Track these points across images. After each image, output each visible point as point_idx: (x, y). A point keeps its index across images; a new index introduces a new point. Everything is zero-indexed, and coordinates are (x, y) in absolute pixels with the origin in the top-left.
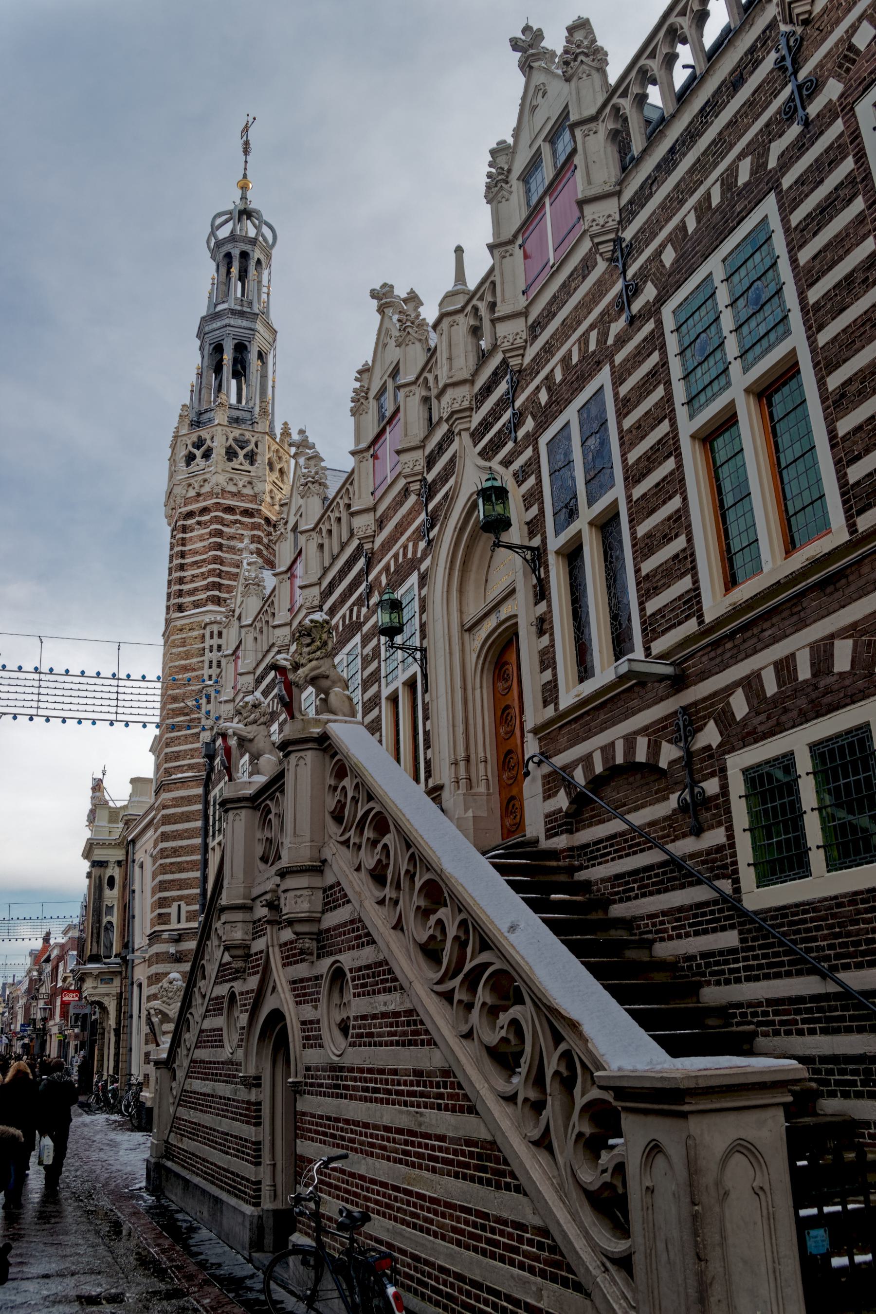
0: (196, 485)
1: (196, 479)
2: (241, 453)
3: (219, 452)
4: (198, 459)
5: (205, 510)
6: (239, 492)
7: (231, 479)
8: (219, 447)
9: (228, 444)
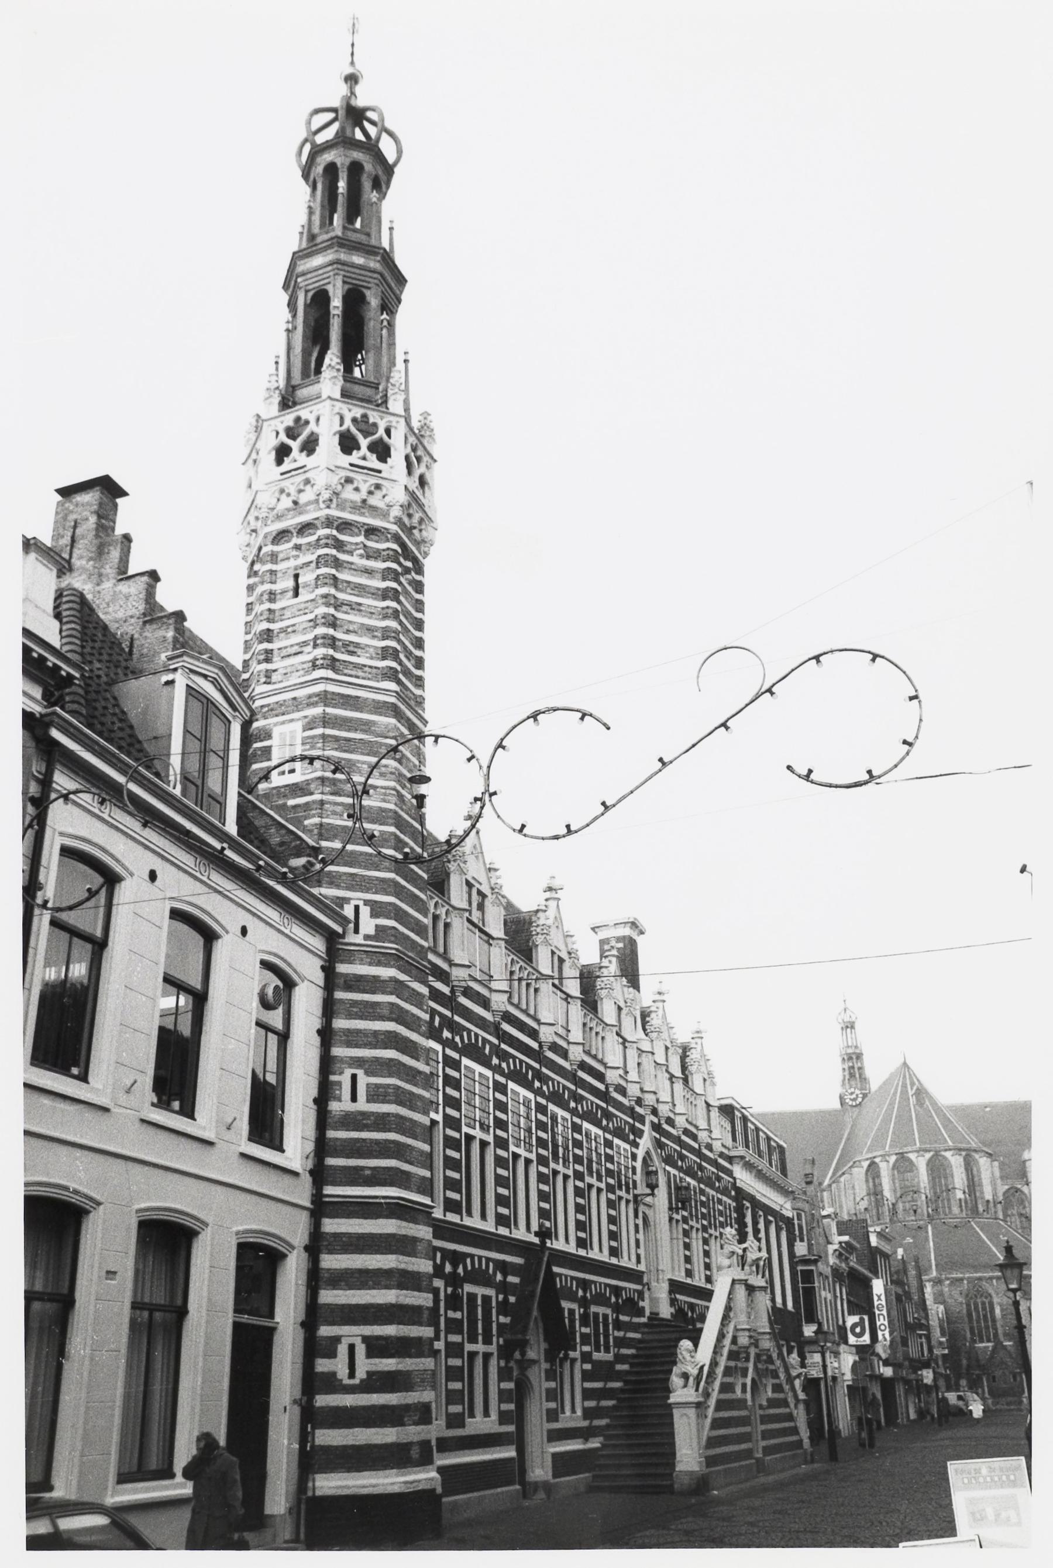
0: (292, 490)
1: (292, 480)
2: (364, 443)
4: (295, 453)
5: (305, 528)
6: (364, 501)
7: (349, 480)
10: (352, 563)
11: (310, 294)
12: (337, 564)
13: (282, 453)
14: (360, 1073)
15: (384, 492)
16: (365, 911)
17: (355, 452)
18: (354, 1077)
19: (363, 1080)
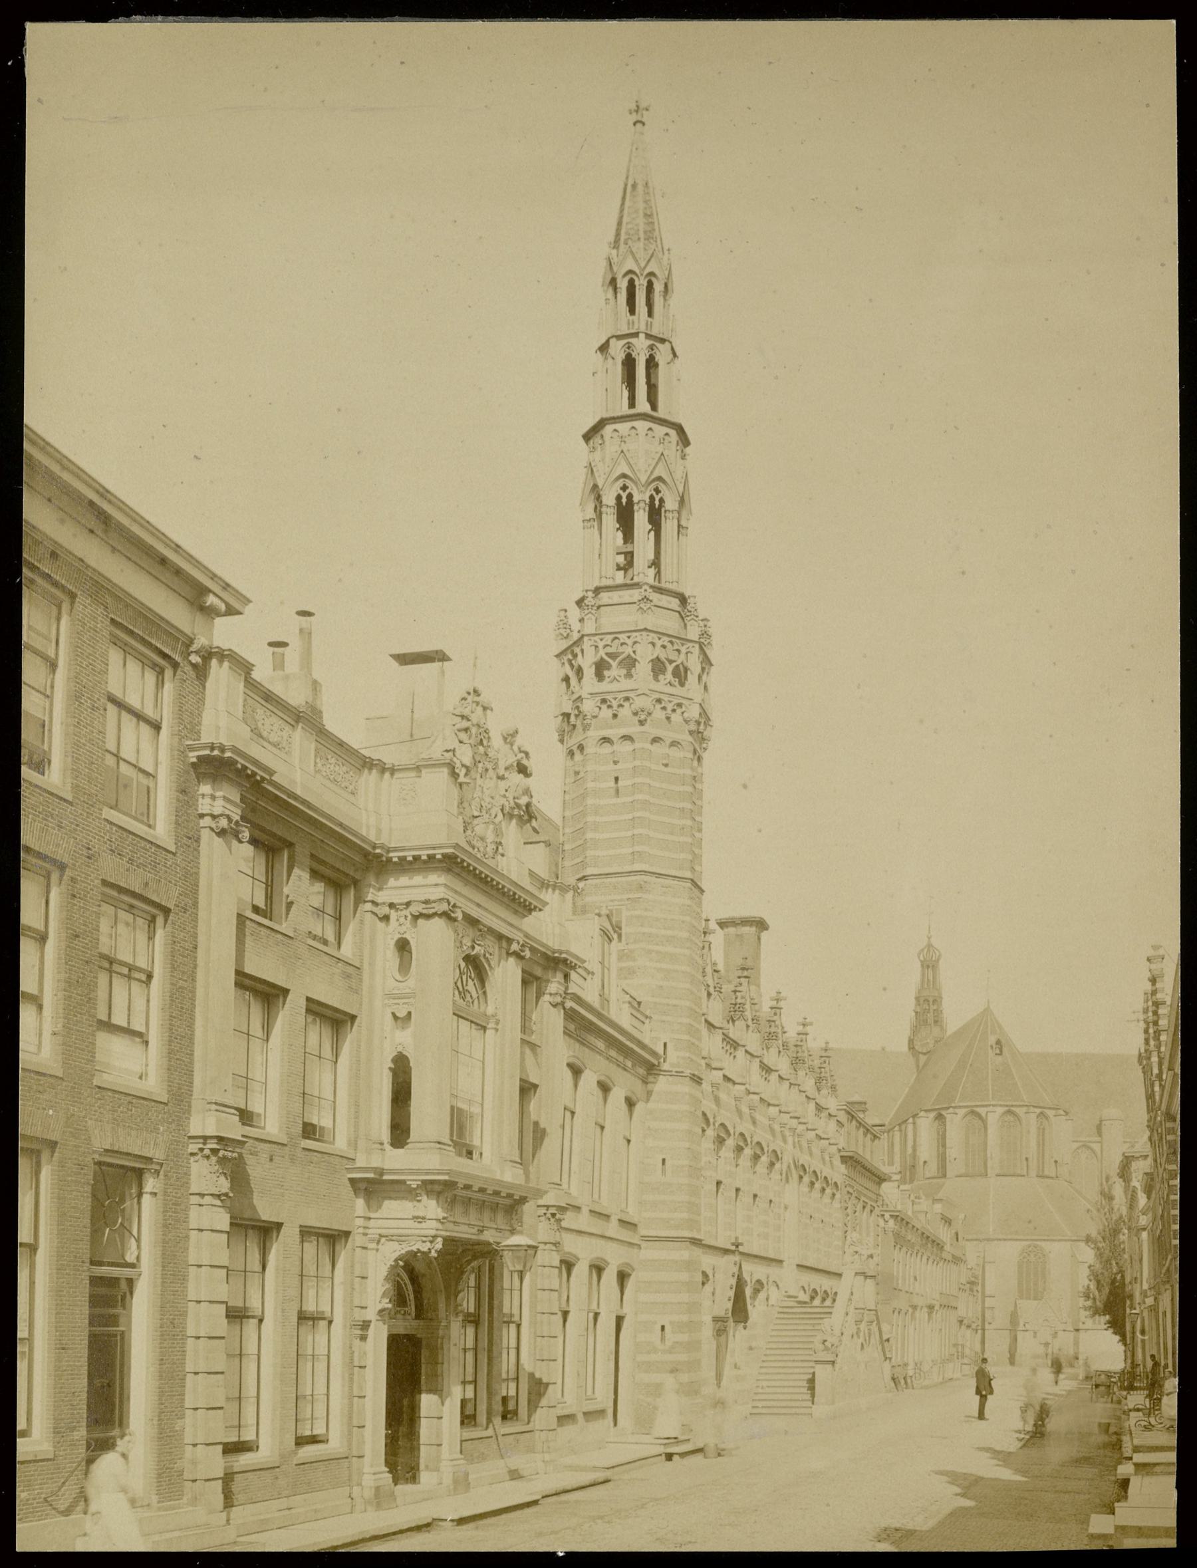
0: (615, 704)
3: (643, 669)
13: (601, 668)
17: (661, 677)
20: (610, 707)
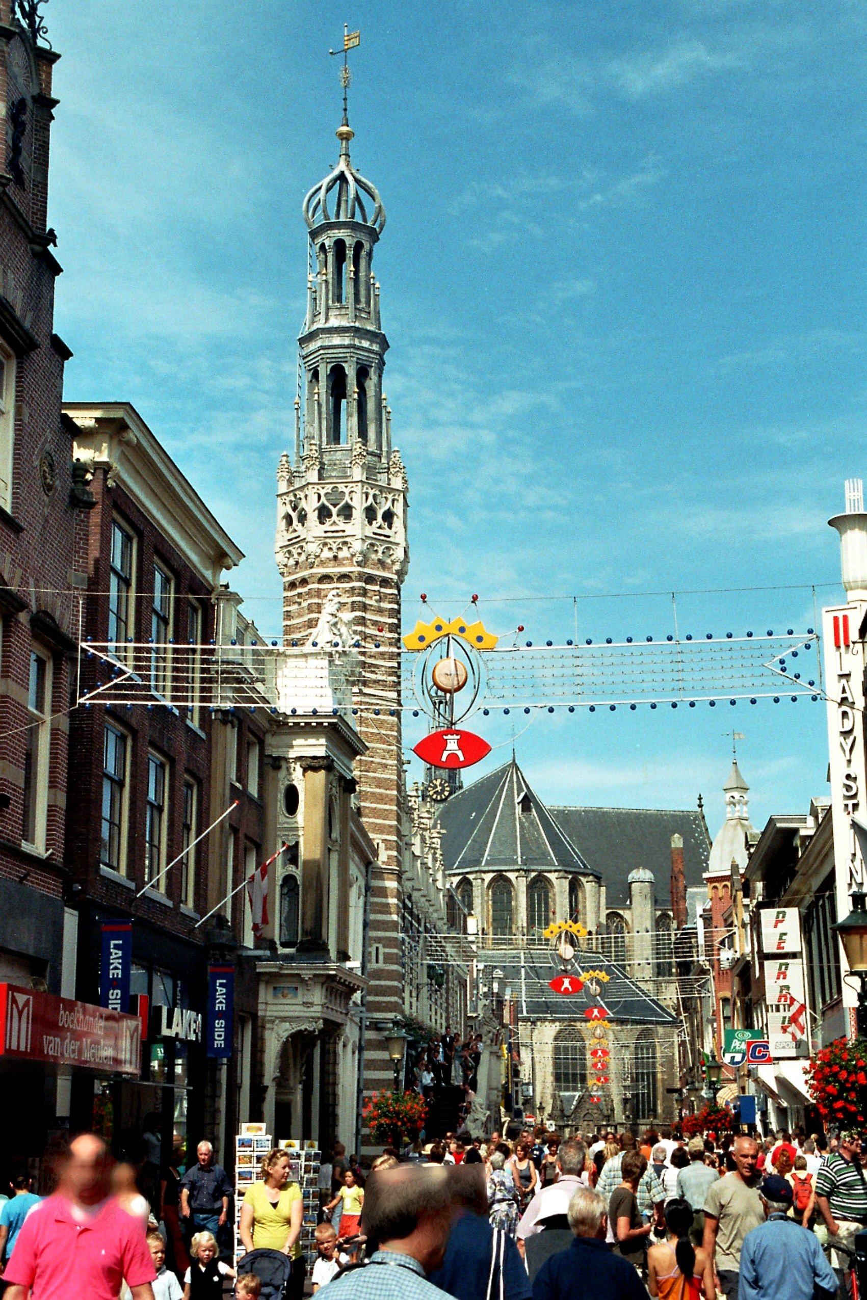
0: (334, 546)
3: (358, 514)
5: (344, 577)
8: (359, 505)
9: (369, 503)
10: (371, 606)
11: (330, 366)
12: (365, 607)
13: (324, 514)
14: (380, 946)
15: (391, 552)
16: (382, 846)
17: (374, 522)
18: (377, 949)
19: (382, 950)
20: (330, 549)
